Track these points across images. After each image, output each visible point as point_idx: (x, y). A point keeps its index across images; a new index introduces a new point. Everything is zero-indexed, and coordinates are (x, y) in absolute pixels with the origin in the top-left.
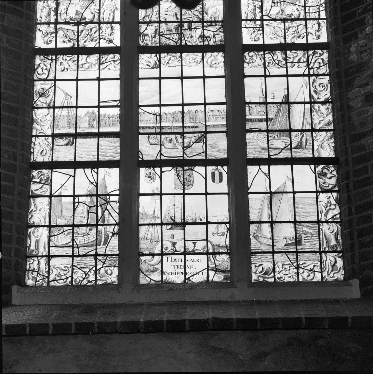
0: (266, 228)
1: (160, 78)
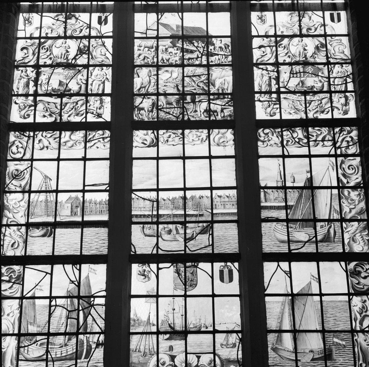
0: (287, 338)
1: (158, 158)
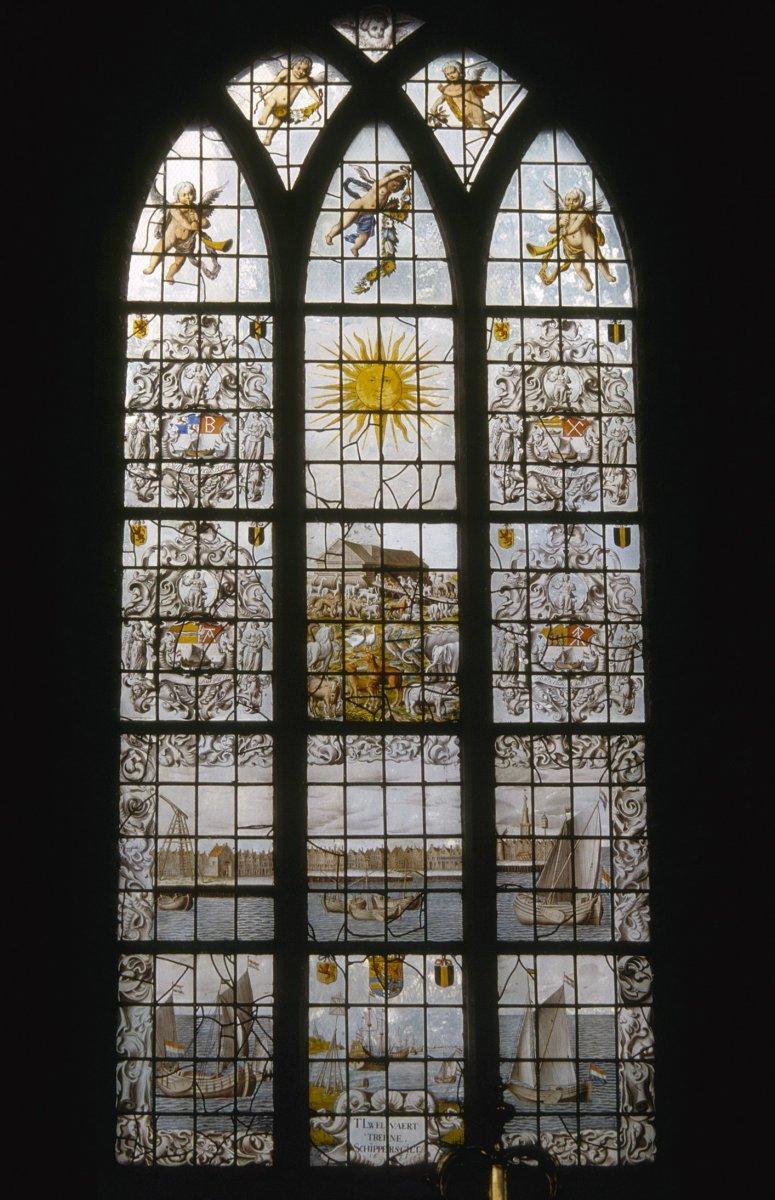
0: (528, 1069)
1: (345, 784)
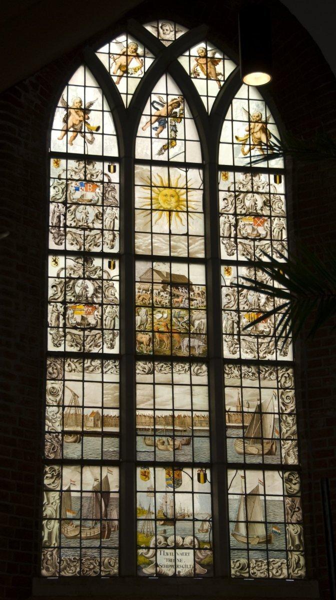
0: (242, 526)
1: (154, 384)
